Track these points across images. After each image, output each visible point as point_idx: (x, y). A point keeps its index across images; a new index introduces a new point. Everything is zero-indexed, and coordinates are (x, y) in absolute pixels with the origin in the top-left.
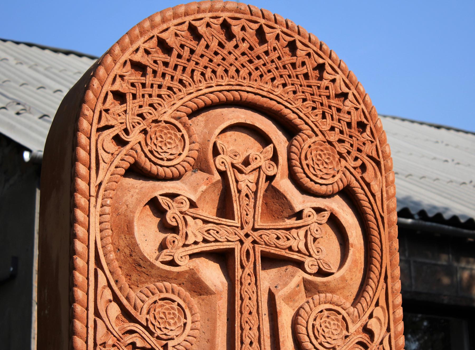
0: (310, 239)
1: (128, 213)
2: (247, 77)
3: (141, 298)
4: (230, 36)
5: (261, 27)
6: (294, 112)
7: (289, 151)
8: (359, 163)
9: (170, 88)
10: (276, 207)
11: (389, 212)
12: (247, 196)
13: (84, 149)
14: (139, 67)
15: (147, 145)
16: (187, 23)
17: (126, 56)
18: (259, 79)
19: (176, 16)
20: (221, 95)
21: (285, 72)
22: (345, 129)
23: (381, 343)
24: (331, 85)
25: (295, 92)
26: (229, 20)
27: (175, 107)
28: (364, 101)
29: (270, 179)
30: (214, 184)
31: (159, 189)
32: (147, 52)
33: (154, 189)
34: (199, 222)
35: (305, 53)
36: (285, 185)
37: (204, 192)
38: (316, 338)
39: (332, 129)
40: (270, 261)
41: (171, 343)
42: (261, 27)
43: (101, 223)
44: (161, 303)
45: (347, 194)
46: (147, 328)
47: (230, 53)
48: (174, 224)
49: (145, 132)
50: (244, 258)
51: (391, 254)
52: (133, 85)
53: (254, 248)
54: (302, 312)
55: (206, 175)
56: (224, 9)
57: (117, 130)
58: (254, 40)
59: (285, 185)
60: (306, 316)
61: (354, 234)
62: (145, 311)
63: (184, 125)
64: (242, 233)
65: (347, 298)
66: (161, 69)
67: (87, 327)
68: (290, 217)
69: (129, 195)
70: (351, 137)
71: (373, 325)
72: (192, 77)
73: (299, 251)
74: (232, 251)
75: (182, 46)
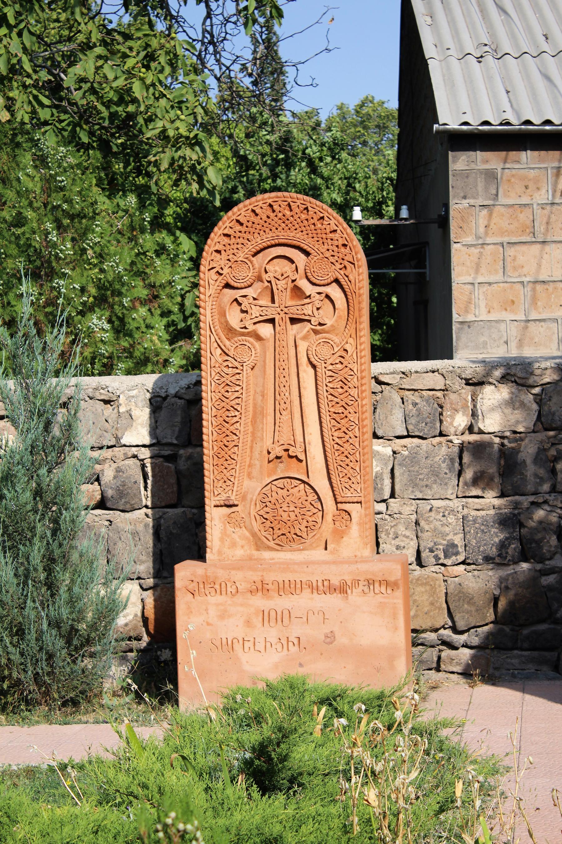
17: (220, 232)
22: (336, 249)
31: (237, 294)
40: (294, 321)
61: (339, 302)
64: (279, 310)
71: (347, 347)
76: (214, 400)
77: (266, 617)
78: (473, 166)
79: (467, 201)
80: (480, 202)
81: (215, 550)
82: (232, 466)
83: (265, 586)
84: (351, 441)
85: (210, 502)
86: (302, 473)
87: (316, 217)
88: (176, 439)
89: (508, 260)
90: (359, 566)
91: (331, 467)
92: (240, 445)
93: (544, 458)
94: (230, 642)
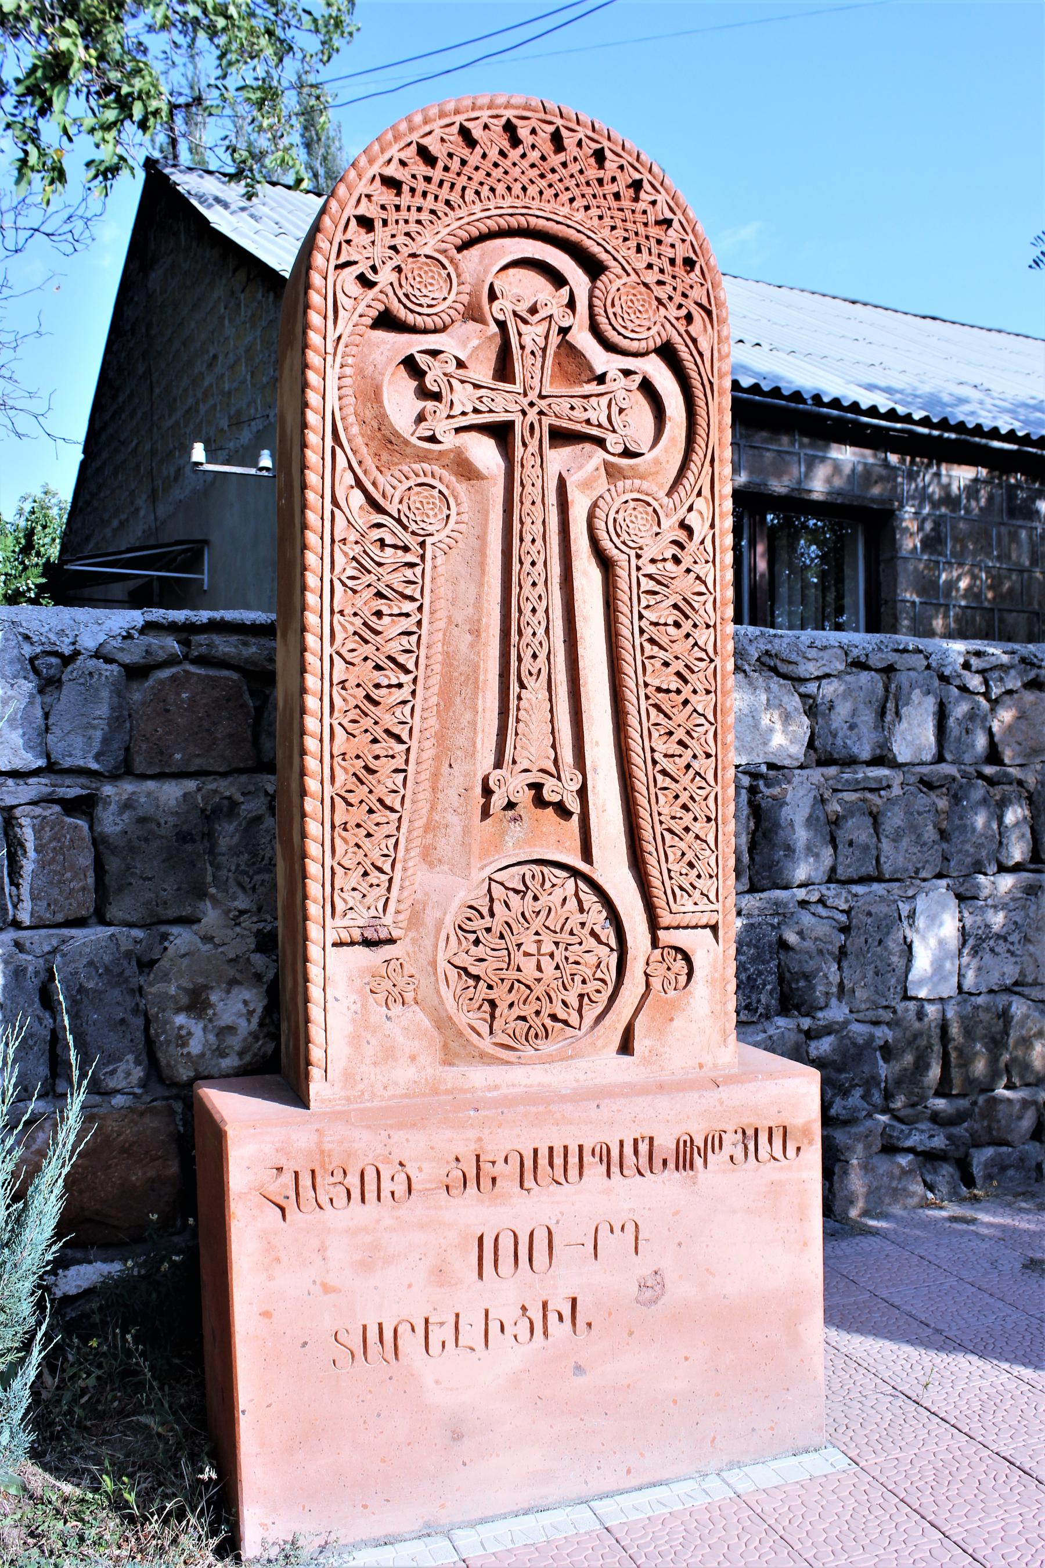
0: (615, 410)
1: (377, 376)
2: (537, 196)
4: (515, 142)
5: (558, 129)
6: (599, 244)
7: (591, 296)
8: (683, 312)
9: (433, 212)
10: (571, 368)
11: (720, 377)
12: (532, 353)
13: (318, 292)
14: (392, 184)
15: (401, 286)
16: (457, 125)
17: (375, 169)
18: (552, 200)
19: (442, 115)
20: (501, 221)
21: (588, 191)
23: (702, 542)
24: (650, 209)
25: (601, 218)
26: (514, 121)
27: (439, 237)
28: (693, 230)
29: (564, 331)
30: (490, 338)
32: (403, 164)
33: (410, 345)
34: (469, 387)
35: (616, 165)
36: (583, 339)
37: (476, 348)
38: (618, 536)
39: (650, 266)
40: (561, 437)
41: (429, 540)
42: (558, 129)
43: (339, 389)
44: (418, 489)
45: (667, 353)
46: (399, 521)
47: (514, 164)
48: (436, 389)
49: (399, 269)
50: (527, 434)
51: (721, 430)
52: (383, 207)
53: (540, 421)
54: (601, 502)
55: (479, 326)
56: (508, 106)
57: (363, 268)
58: (548, 148)
59: (583, 339)
60: (606, 508)
61: (673, 405)
62: (396, 500)
63: (452, 261)
64: (525, 402)
65: (661, 486)
66: (421, 186)
67: (322, 519)
68: (589, 382)
69: (378, 352)
70: (674, 277)
71: (692, 520)
72: (463, 197)
73: (600, 426)
74: (512, 423)
75: (450, 155)
76: (340, 636)
77: (485, 1253)
82: (386, 830)
83: (486, 1167)
84: (696, 764)
85: (319, 932)
86: (569, 850)
87: (624, 179)
88: (97, 758)
90: (724, 1093)
91: (647, 834)
92: (411, 768)
94: (388, 1335)
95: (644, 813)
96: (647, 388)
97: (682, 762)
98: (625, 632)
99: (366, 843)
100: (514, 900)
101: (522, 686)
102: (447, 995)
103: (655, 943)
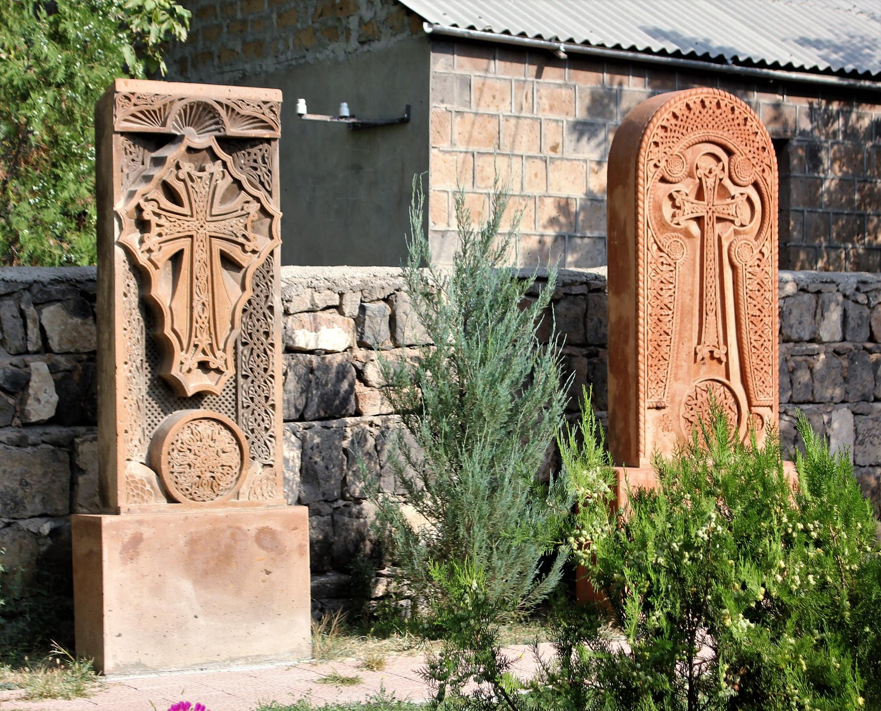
3: (663, 239)
4: (704, 106)
10: (722, 193)
14: (664, 128)
17: (660, 123)
21: (729, 124)
29: (721, 180)
33: (670, 189)
36: (727, 182)
40: (719, 220)
41: (677, 262)
45: (756, 185)
55: (692, 180)
59: (727, 182)
71: (764, 250)
74: (703, 217)
78: (450, 70)
79: (444, 106)
80: (455, 107)
81: (648, 454)
84: (765, 344)
85: (644, 403)
89: (477, 169)
91: (748, 370)
93: (786, 369)
95: (747, 362)
96: (749, 200)
97: (760, 343)
98: (741, 294)
99: (658, 372)
100: (704, 393)
101: (707, 314)
102: (682, 426)
103: (750, 410)
